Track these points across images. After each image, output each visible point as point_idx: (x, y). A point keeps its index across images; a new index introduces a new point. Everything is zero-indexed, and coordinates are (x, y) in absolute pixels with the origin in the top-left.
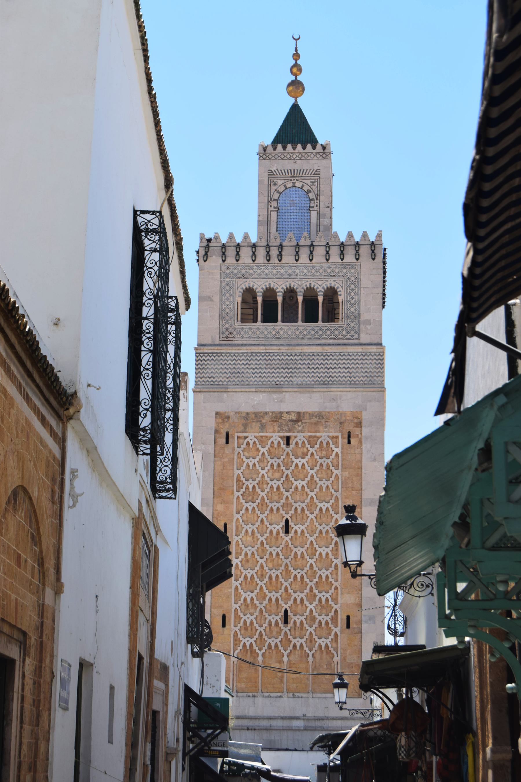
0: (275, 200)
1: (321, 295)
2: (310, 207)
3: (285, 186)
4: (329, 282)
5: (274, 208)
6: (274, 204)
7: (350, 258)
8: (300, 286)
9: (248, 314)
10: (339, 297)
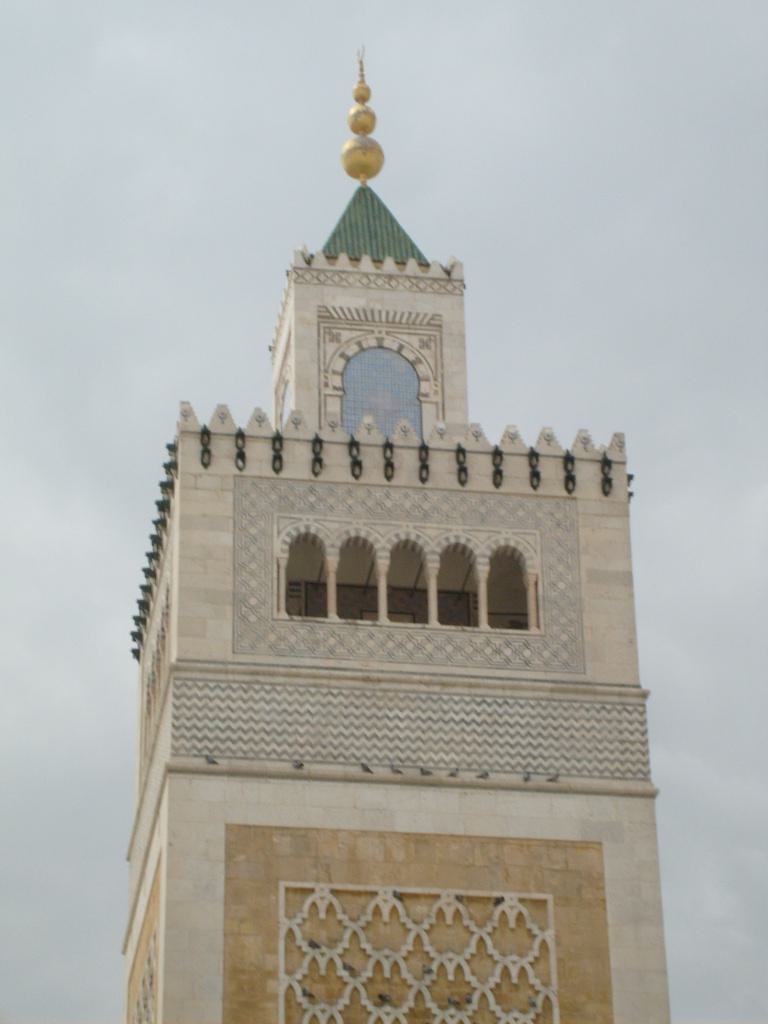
0: (334, 372)
4: (504, 535)
5: (335, 388)
6: (337, 381)
8: (433, 541)
9: (305, 596)
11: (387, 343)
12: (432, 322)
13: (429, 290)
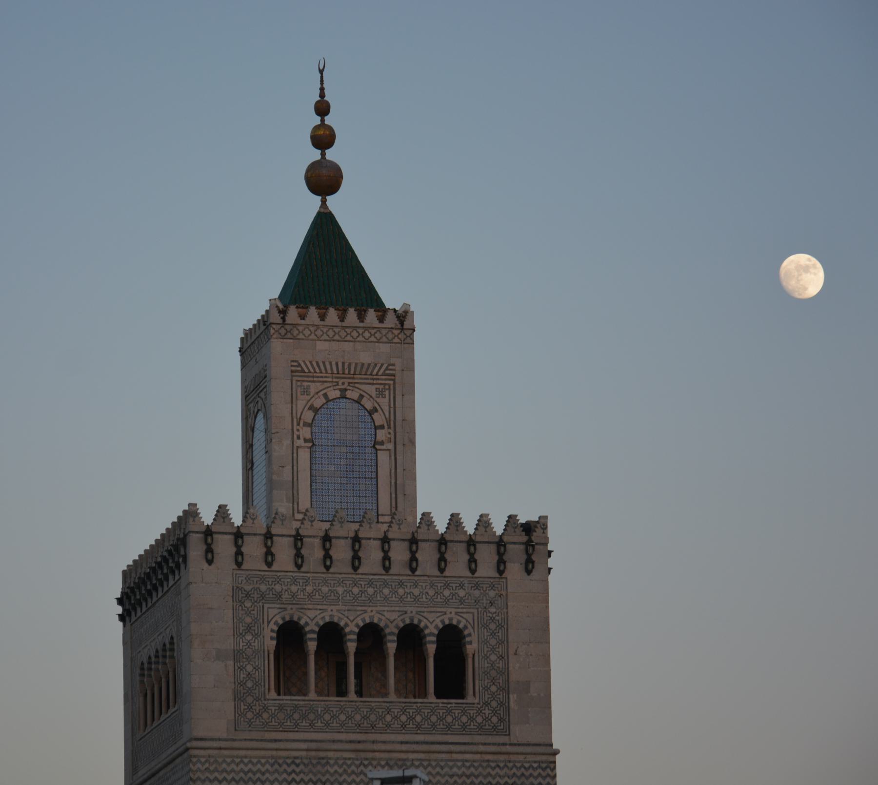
1: (432, 642)
2: (376, 443)
3: (325, 395)
4: (449, 616)
6: (306, 432)
7: (486, 568)
10: (468, 647)
11: (349, 394)
12: (388, 372)
13: (384, 339)
